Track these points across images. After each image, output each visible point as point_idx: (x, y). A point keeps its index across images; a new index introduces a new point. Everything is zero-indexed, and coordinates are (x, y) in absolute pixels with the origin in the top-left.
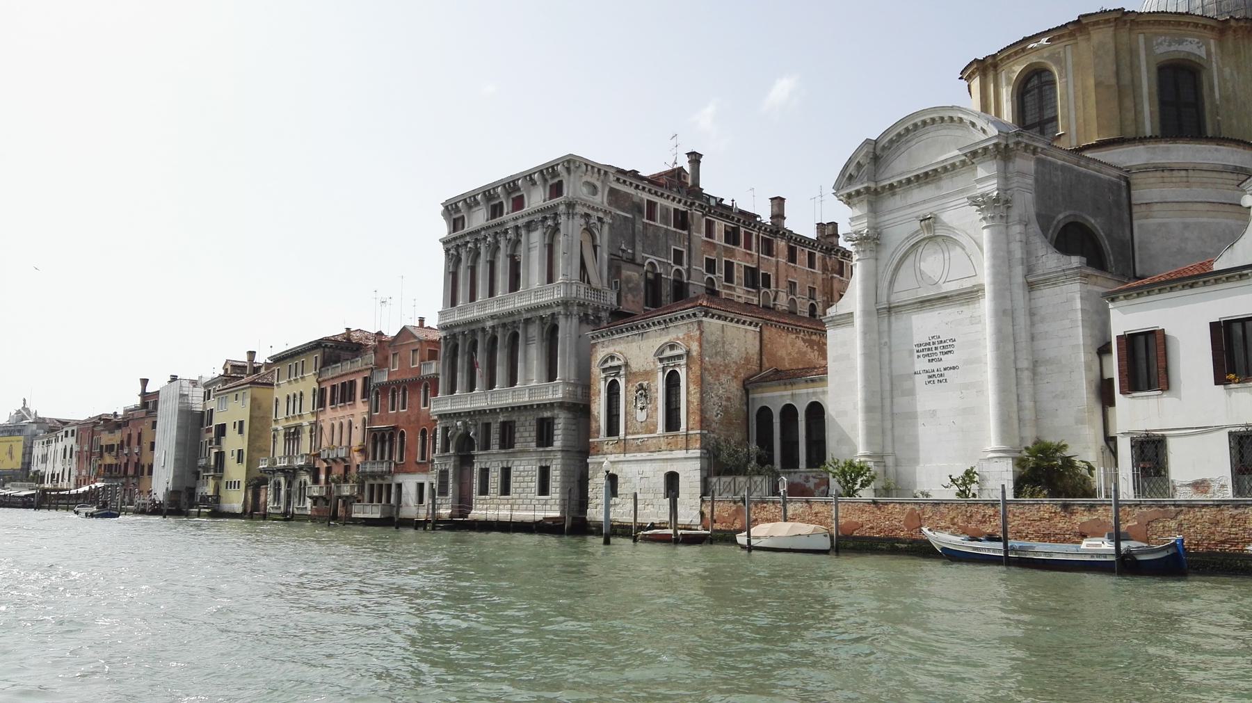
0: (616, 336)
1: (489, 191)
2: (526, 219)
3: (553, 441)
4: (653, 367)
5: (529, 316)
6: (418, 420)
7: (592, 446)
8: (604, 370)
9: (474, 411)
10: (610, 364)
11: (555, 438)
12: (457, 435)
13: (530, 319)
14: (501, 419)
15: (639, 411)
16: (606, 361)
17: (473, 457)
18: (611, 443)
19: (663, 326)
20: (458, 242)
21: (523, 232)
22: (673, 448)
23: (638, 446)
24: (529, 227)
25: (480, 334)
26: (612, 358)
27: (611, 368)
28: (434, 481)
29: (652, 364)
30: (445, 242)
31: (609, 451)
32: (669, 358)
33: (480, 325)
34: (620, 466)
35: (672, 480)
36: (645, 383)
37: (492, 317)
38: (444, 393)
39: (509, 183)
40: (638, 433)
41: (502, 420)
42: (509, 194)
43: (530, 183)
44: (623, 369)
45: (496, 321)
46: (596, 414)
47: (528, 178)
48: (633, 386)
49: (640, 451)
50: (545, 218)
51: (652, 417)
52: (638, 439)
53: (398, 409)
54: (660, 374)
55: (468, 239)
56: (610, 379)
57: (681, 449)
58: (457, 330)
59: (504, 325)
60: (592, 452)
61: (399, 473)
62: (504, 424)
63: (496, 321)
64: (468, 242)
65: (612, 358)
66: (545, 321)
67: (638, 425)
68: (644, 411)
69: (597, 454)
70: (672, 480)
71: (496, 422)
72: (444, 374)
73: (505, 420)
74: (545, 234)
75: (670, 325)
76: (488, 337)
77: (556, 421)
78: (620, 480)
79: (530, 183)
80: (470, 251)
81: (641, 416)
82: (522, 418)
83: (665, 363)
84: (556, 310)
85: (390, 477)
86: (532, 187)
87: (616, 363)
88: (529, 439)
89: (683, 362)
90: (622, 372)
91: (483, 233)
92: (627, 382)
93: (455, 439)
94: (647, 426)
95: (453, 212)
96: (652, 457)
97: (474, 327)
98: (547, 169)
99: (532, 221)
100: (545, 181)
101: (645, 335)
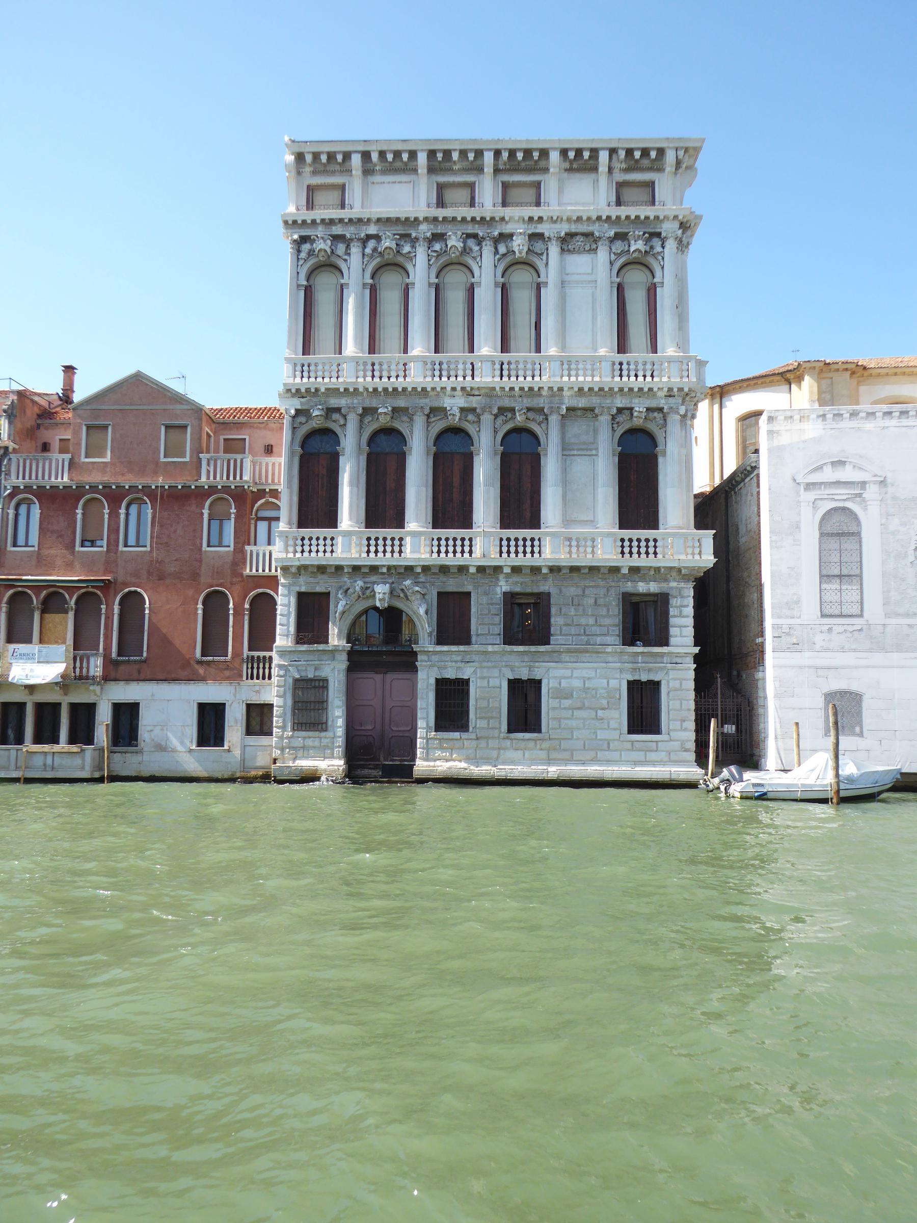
1: (447, 153)
2: (564, 228)
5: (582, 403)
9: (426, 569)
11: (673, 631)
12: (360, 606)
13: (592, 410)
14: (504, 586)
17: (415, 654)
20: (337, 230)
21: (554, 250)
24: (566, 241)
25: (419, 421)
28: (276, 701)
30: (291, 224)
33: (427, 403)
37: (467, 392)
38: (290, 523)
39: (512, 153)
41: (506, 588)
42: (497, 171)
43: (567, 165)
45: (474, 402)
47: (571, 155)
50: (621, 237)
53: (113, 544)
55: (372, 230)
58: (342, 402)
59: (502, 410)
62: (510, 598)
64: (377, 238)
66: (620, 419)
71: (486, 593)
72: (289, 486)
73: (518, 589)
74: (611, 263)
76: (439, 426)
77: (673, 602)
79: (567, 165)
80: (372, 256)
82: (572, 591)
84: (662, 403)
85: (97, 689)
86: (566, 175)
91: (423, 227)
93: (350, 618)
95: (308, 169)
97: (401, 403)
98: (629, 152)
99: (576, 234)
100: (610, 170)
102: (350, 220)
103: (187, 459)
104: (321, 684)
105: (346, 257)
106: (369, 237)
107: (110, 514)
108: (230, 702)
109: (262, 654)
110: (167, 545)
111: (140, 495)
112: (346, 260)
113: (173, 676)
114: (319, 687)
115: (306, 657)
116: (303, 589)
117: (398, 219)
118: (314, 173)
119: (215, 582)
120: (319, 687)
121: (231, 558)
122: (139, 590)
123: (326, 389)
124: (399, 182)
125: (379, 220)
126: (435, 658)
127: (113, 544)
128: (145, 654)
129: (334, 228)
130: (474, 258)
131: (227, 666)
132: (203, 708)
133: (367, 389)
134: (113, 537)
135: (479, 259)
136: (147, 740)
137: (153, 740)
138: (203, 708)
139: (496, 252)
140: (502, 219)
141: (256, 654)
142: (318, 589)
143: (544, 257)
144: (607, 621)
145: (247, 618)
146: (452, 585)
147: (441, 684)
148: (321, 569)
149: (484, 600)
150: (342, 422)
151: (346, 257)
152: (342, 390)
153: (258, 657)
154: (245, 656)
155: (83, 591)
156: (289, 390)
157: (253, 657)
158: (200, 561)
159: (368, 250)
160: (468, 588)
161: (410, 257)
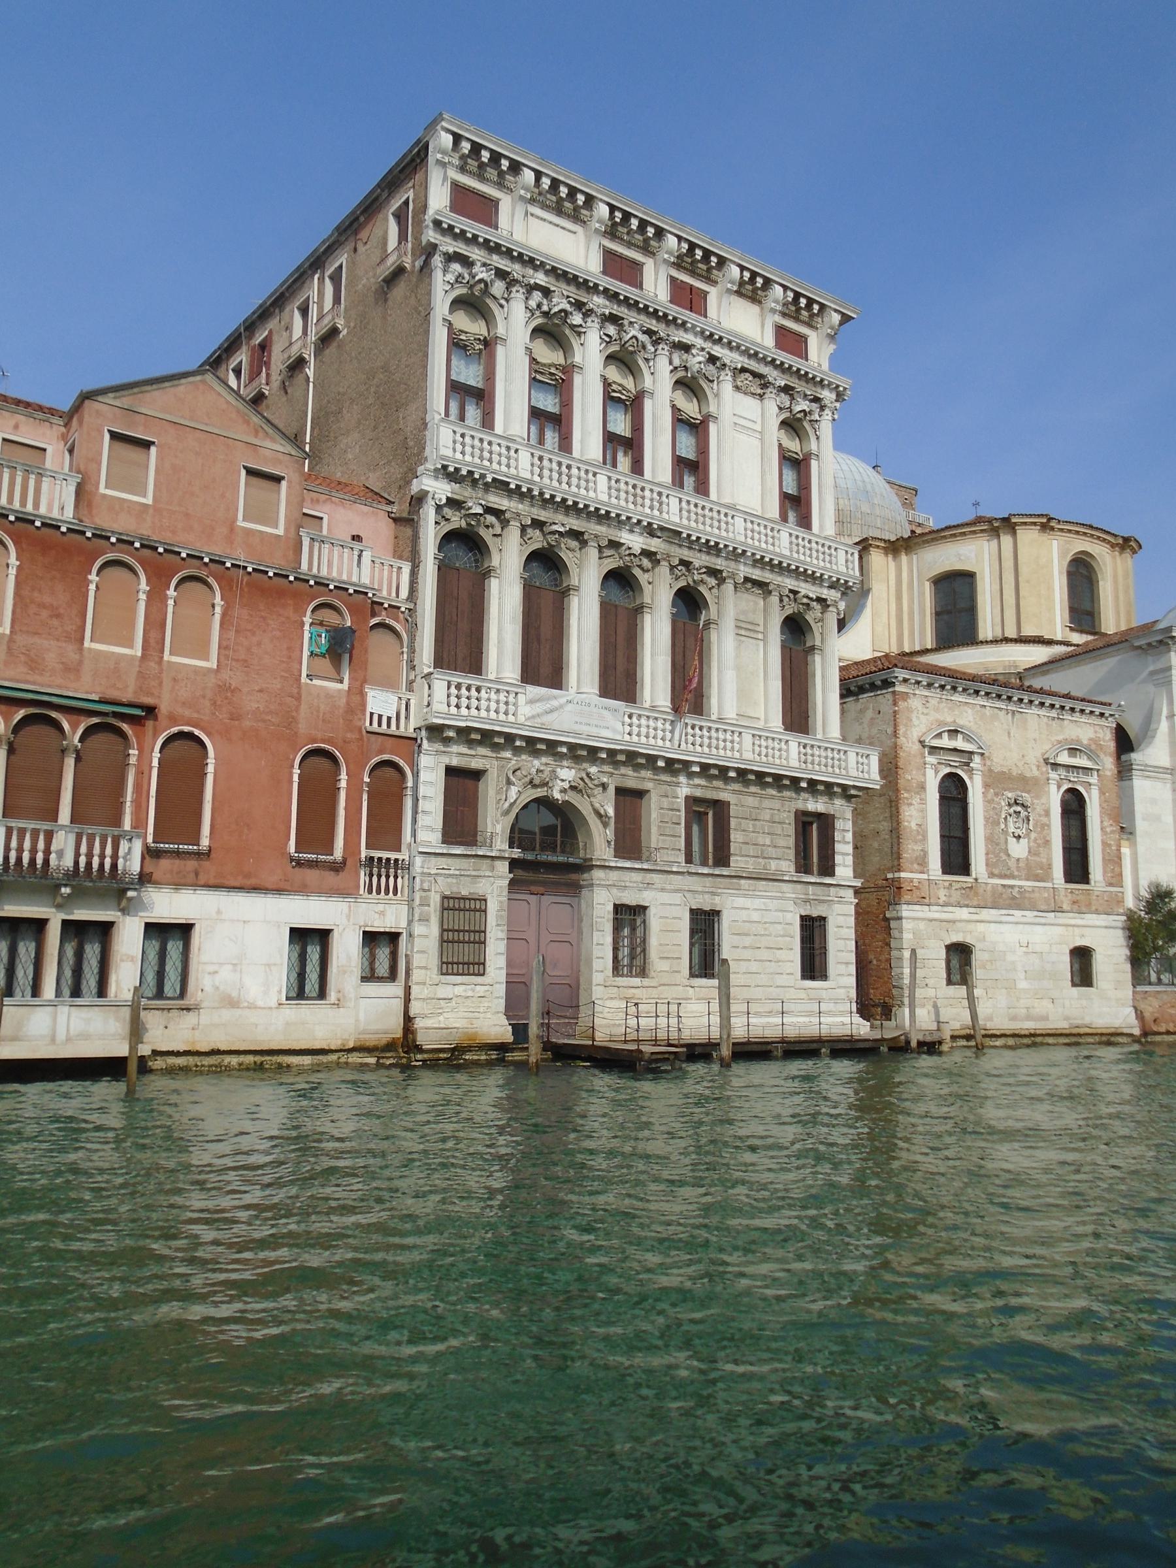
0: (957, 697)
3: (833, 866)
4: (1036, 773)
5: (757, 574)
6: (290, 721)
7: (906, 886)
8: (934, 750)
10: (945, 742)
15: (1012, 840)
16: (939, 735)
18: (956, 886)
19: (1054, 713)
22: (1084, 909)
23: (1014, 898)
26: (954, 733)
27: (955, 750)
29: (1034, 768)
31: (953, 900)
32: (1068, 767)
34: (981, 927)
35: (1082, 957)
36: (1027, 798)
40: (1013, 877)
44: (977, 759)
46: (913, 825)
48: (996, 794)
49: (1019, 907)
51: (1037, 854)
52: (1012, 887)
53: (154, 646)
54: (1053, 787)
55: (540, 278)
56: (948, 770)
57: (1097, 912)
60: (906, 897)
61: (178, 884)
63: (655, 544)
64: (546, 292)
65: (954, 733)
67: (1012, 864)
68: (1024, 841)
69: (922, 901)
70: (1082, 957)
73: (698, 793)
75: (1067, 716)
78: (978, 958)
81: (1018, 850)
83: (1063, 772)
87: (960, 743)
88: (772, 852)
89: (1093, 779)
90: (976, 762)
92: (986, 786)
94: (1028, 867)
96: (1043, 921)
101: (1017, 716)
102: (521, 255)
103: (280, 531)
104: (477, 906)
105: (503, 302)
106: (537, 287)
107: (149, 595)
108: (341, 928)
109: (385, 855)
110: (246, 663)
111: (203, 573)
112: (502, 306)
113: (253, 881)
114: (475, 910)
115: (464, 863)
116: (455, 762)
117: (576, 277)
118: (463, 169)
119: (319, 735)
120: (475, 910)
121: (344, 700)
122: (197, 732)
123: (494, 479)
124: (563, 228)
125: (554, 269)
126: (614, 876)
127: (154, 646)
128: (205, 842)
129: (495, 257)
130: (647, 360)
131: (337, 868)
132: (300, 936)
133: (541, 494)
134: (153, 635)
135: (651, 363)
136: (208, 988)
137: (217, 988)
138: (300, 936)
139: (671, 363)
140: (684, 323)
141: (377, 854)
142: (475, 764)
143: (715, 386)
144: (782, 842)
145: (365, 797)
146: (631, 778)
147: (620, 909)
148: (487, 738)
149: (665, 803)
150: (498, 530)
151: (503, 302)
152: (513, 486)
153: (380, 859)
154: (363, 855)
155: (95, 720)
156: (445, 467)
157: (372, 858)
158: (298, 698)
159: (533, 303)
160: (649, 785)
161: (578, 331)
